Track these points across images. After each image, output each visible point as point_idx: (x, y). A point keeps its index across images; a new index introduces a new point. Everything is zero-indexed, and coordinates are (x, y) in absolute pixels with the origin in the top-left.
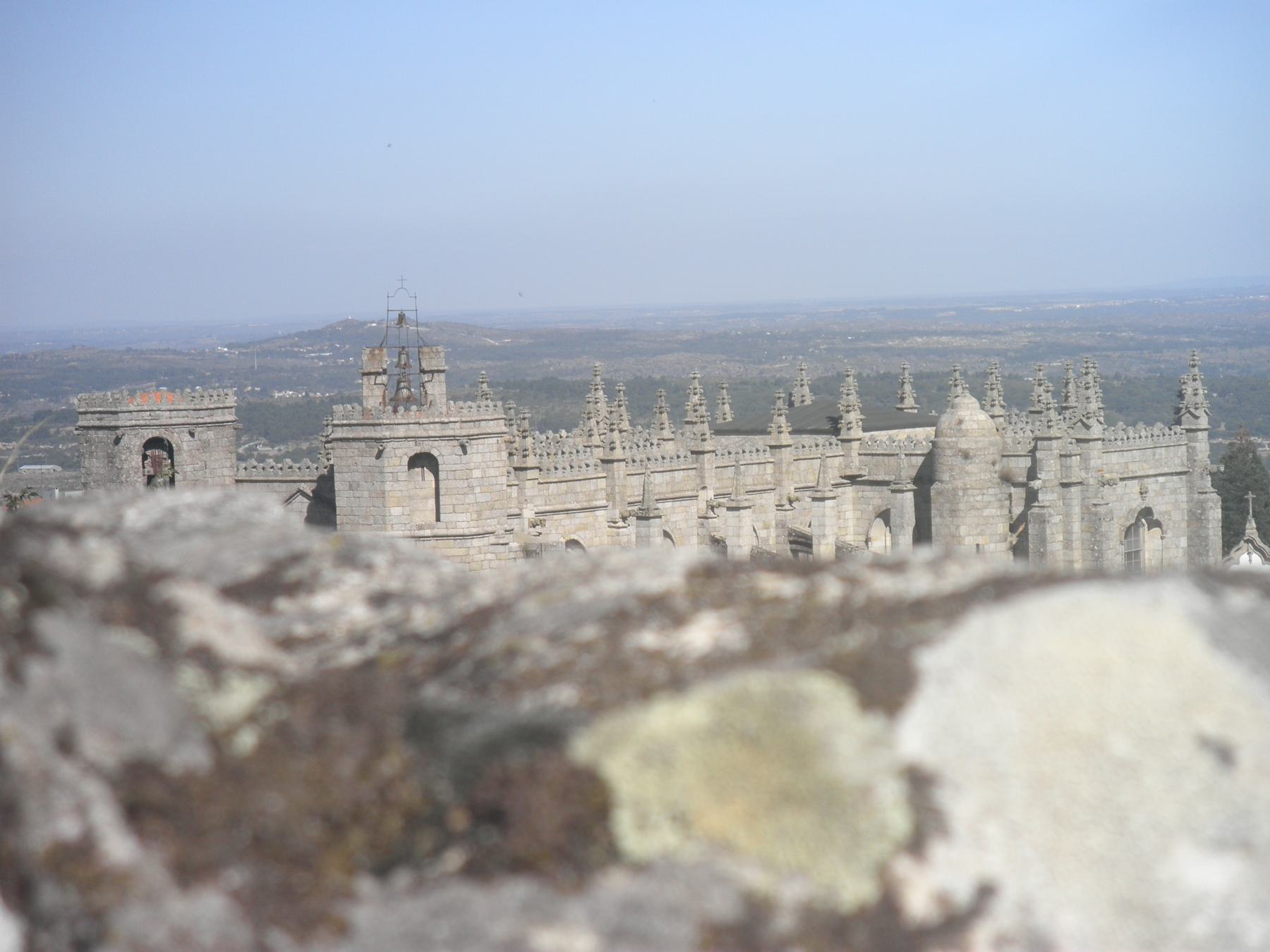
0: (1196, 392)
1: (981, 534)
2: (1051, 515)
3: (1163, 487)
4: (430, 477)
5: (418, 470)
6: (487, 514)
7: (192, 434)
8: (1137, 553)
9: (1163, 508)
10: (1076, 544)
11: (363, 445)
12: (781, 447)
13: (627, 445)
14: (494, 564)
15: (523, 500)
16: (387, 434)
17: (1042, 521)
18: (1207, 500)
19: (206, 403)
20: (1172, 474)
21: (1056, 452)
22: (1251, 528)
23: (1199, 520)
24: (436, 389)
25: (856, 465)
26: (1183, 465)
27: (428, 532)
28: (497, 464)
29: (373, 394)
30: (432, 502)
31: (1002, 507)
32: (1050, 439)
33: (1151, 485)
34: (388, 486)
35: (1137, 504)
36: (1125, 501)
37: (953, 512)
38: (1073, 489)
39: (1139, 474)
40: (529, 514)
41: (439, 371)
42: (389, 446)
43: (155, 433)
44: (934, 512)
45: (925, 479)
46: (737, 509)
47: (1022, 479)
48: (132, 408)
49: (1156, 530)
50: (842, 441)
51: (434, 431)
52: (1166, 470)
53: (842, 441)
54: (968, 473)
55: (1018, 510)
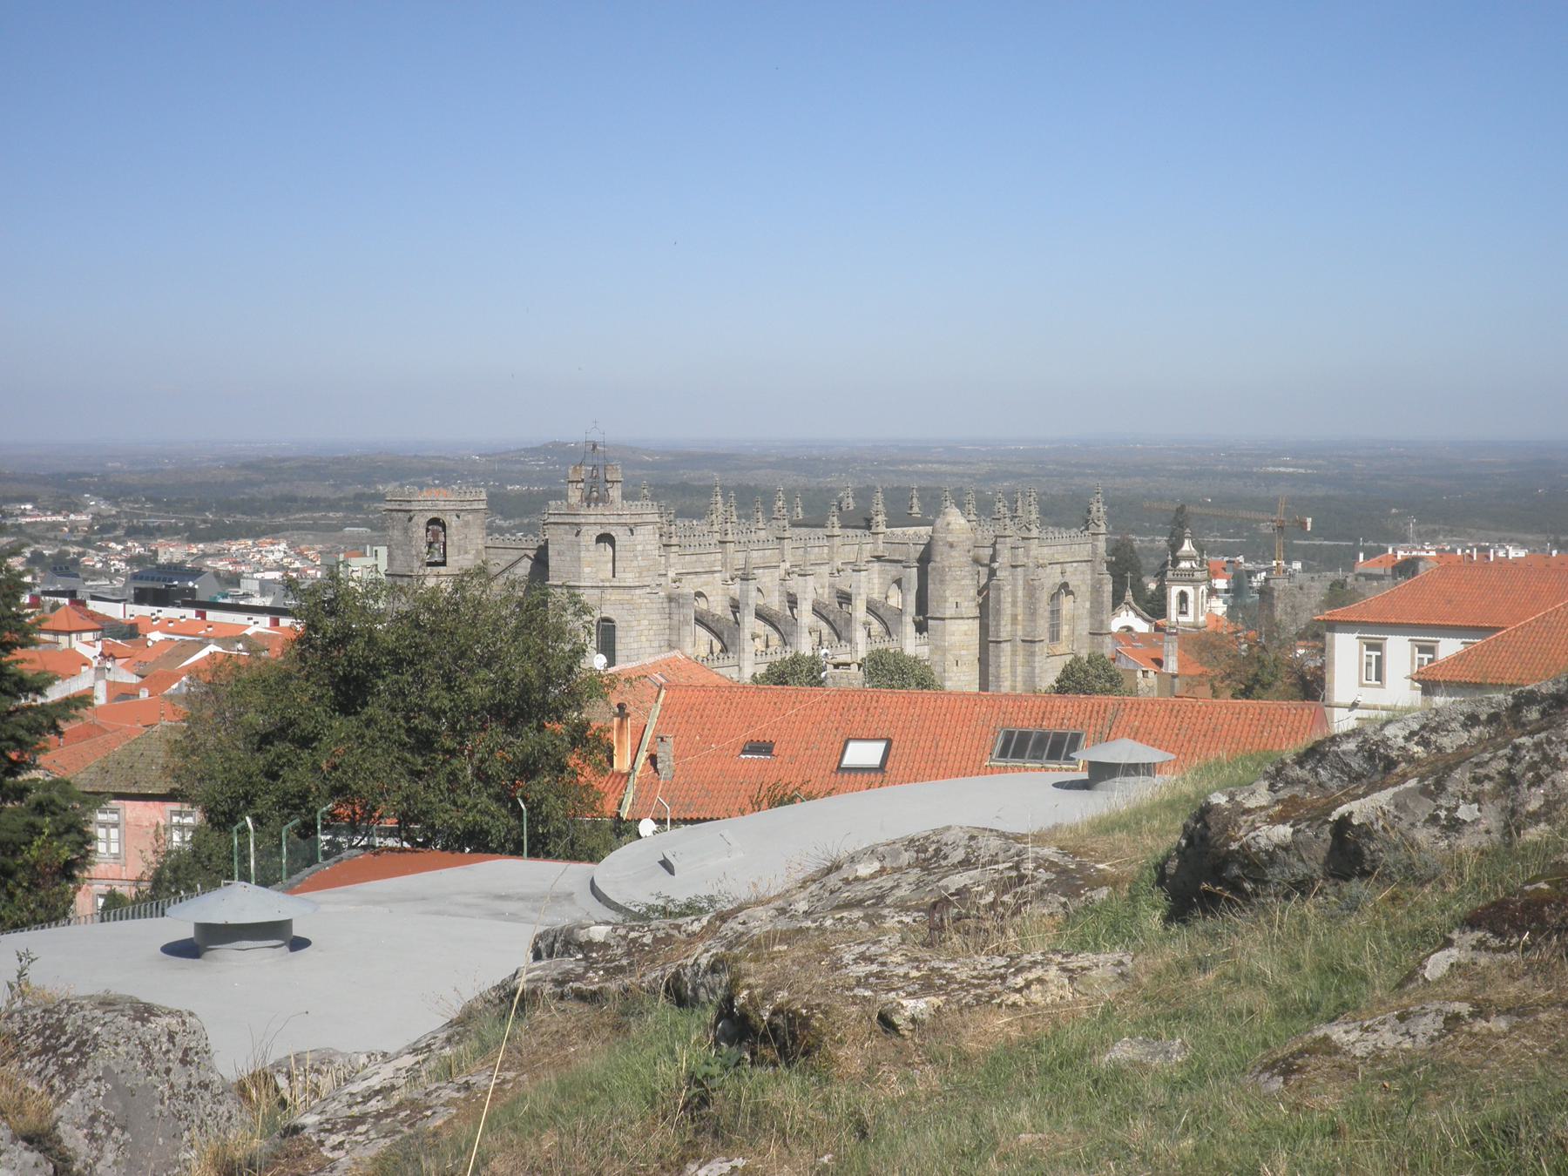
0: (1098, 509)
1: (960, 596)
4: (609, 549)
6: (645, 574)
7: (458, 517)
8: (1058, 610)
9: (1076, 583)
10: (1020, 604)
11: (567, 527)
12: (833, 536)
13: (735, 532)
14: (648, 606)
15: (668, 566)
16: (583, 521)
17: (999, 588)
18: (1103, 579)
19: (468, 497)
20: (1081, 562)
21: (1009, 545)
22: (1129, 595)
23: (1098, 591)
24: (615, 493)
27: (607, 584)
29: (575, 495)
30: (611, 565)
32: (1005, 537)
33: (1069, 568)
34: (582, 554)
35: (1059, 580)
36: (1052, 577)
37: (942, 582)
38: (1019, 569)
40: (672, 574)
41: (617, 481)
42: (584, 529)
43: (435, 515)
44: (929, 581)
45: (925, 559)
46: (805, 575)
47: (987, 562)
48: (420, 498)
51: (613, 520)
52: (1078, 559)
53: (873, 533)
54: (953, 557)
55: (983, 581)
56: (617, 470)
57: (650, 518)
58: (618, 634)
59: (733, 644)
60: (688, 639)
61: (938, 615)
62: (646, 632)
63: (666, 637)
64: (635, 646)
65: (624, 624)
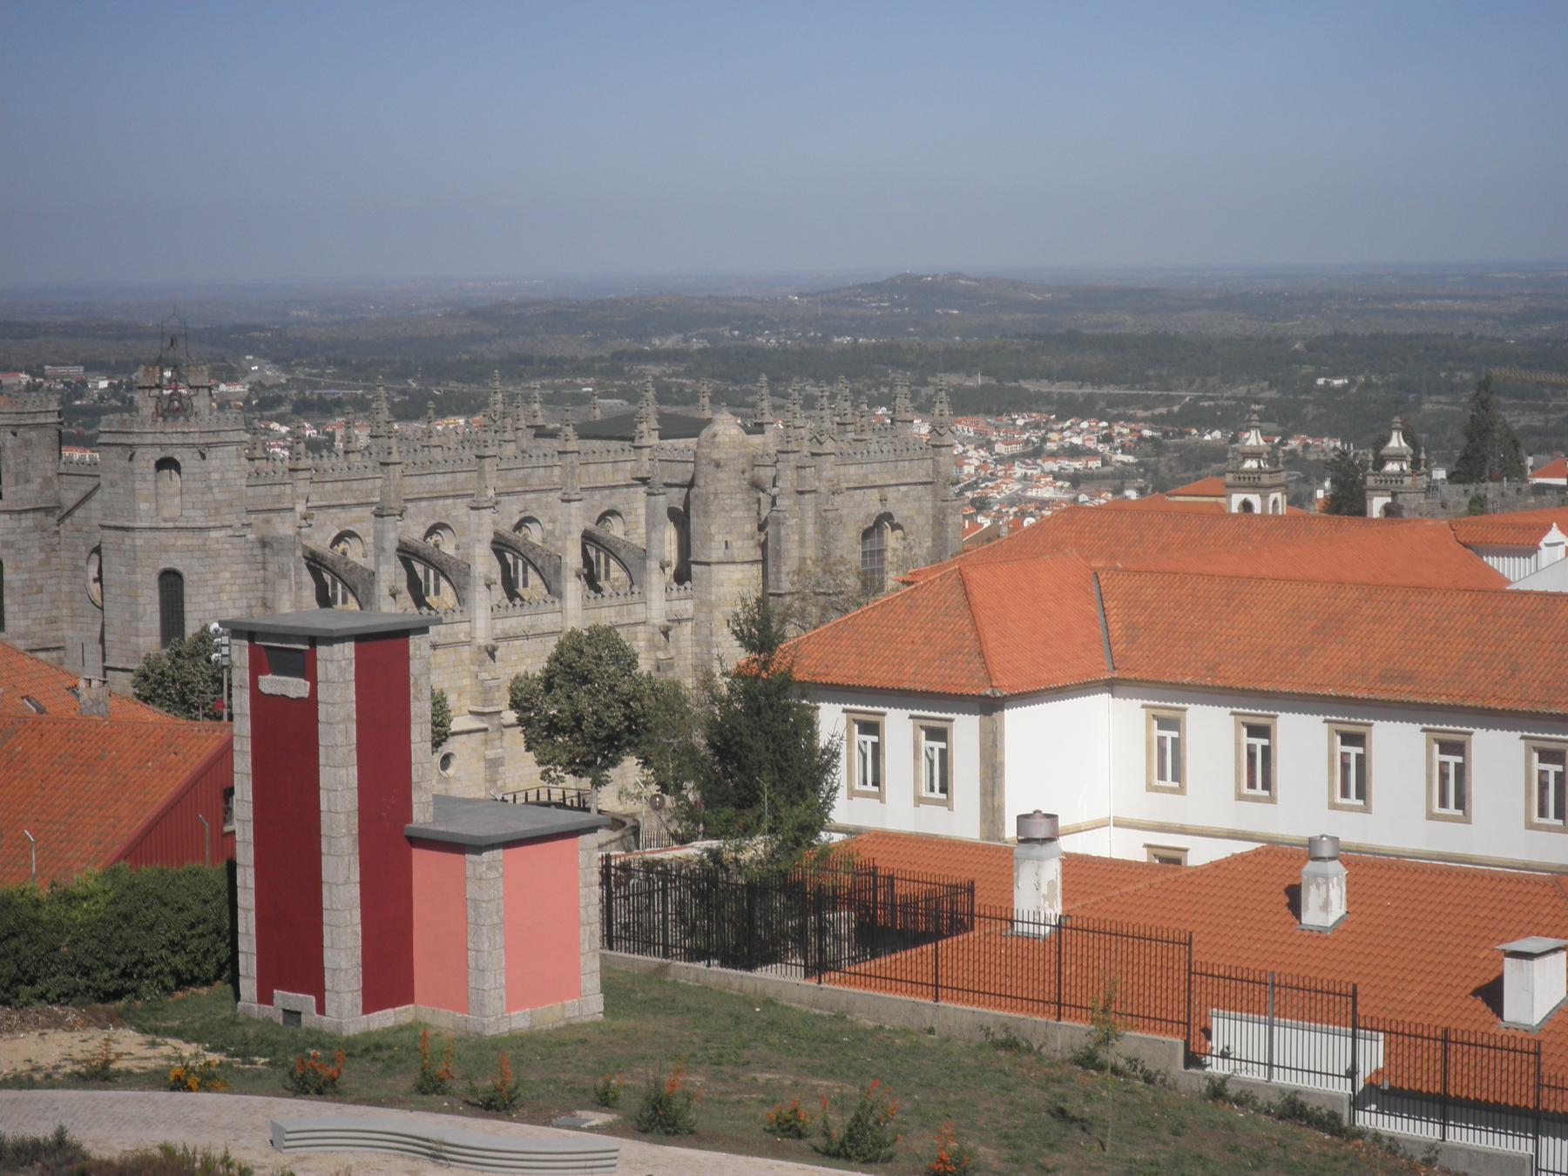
1: (729, 533)
2: (785, 518)
3: (906, 495)
5: (167, 471)
7: (15, 434)
8: (881, 552)
9: (906, 513)
11: (119, 449)
12: (566, 453)
13: (404, 448)
14: (230, 553)
16: (137, 441)
17: (778, 523)
18: (946, 508)
19: (29, 408)
20: (915, 484)
21: (793, 464)
23: (941, 524)
25: (646, 467)
26: (928, 475)
27: (170, 525)
28: (236, 468)
31: (749, 510)
32: (787, 452)
33: (892, 494)
34: (137, 485)
35: (876, 509)
36: (871, 505)
37: (706, 512)
38: (806, 496)
39: (879, 483)
40: (300, 508)
42: (139, 451)
44: (692, 513)
46: (477, 509)
49: (899, 533)
50: (635, 447)
51: (177, 439)
52: (909, 480)
53: (635, 447)
54: (720, 480)
55: (765, 513)
56: (202, 371)
57: (232, 436)
58: (188, 590)
59: (369, 602)
60: (285, 597)
61: (702, 559)
62: (228, 588)
63: (259, 594)
64: (211, 606)
65: (192, 578)
